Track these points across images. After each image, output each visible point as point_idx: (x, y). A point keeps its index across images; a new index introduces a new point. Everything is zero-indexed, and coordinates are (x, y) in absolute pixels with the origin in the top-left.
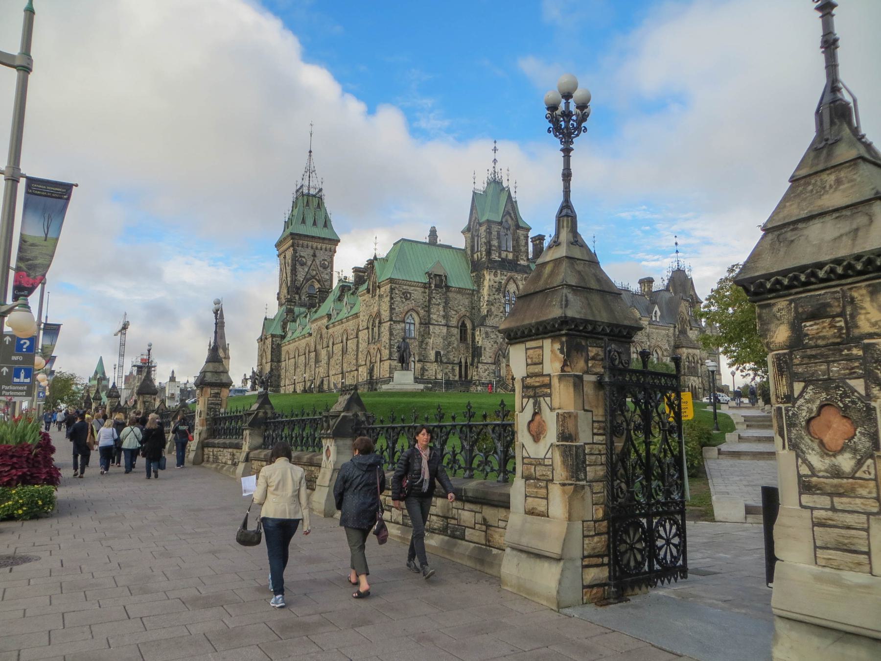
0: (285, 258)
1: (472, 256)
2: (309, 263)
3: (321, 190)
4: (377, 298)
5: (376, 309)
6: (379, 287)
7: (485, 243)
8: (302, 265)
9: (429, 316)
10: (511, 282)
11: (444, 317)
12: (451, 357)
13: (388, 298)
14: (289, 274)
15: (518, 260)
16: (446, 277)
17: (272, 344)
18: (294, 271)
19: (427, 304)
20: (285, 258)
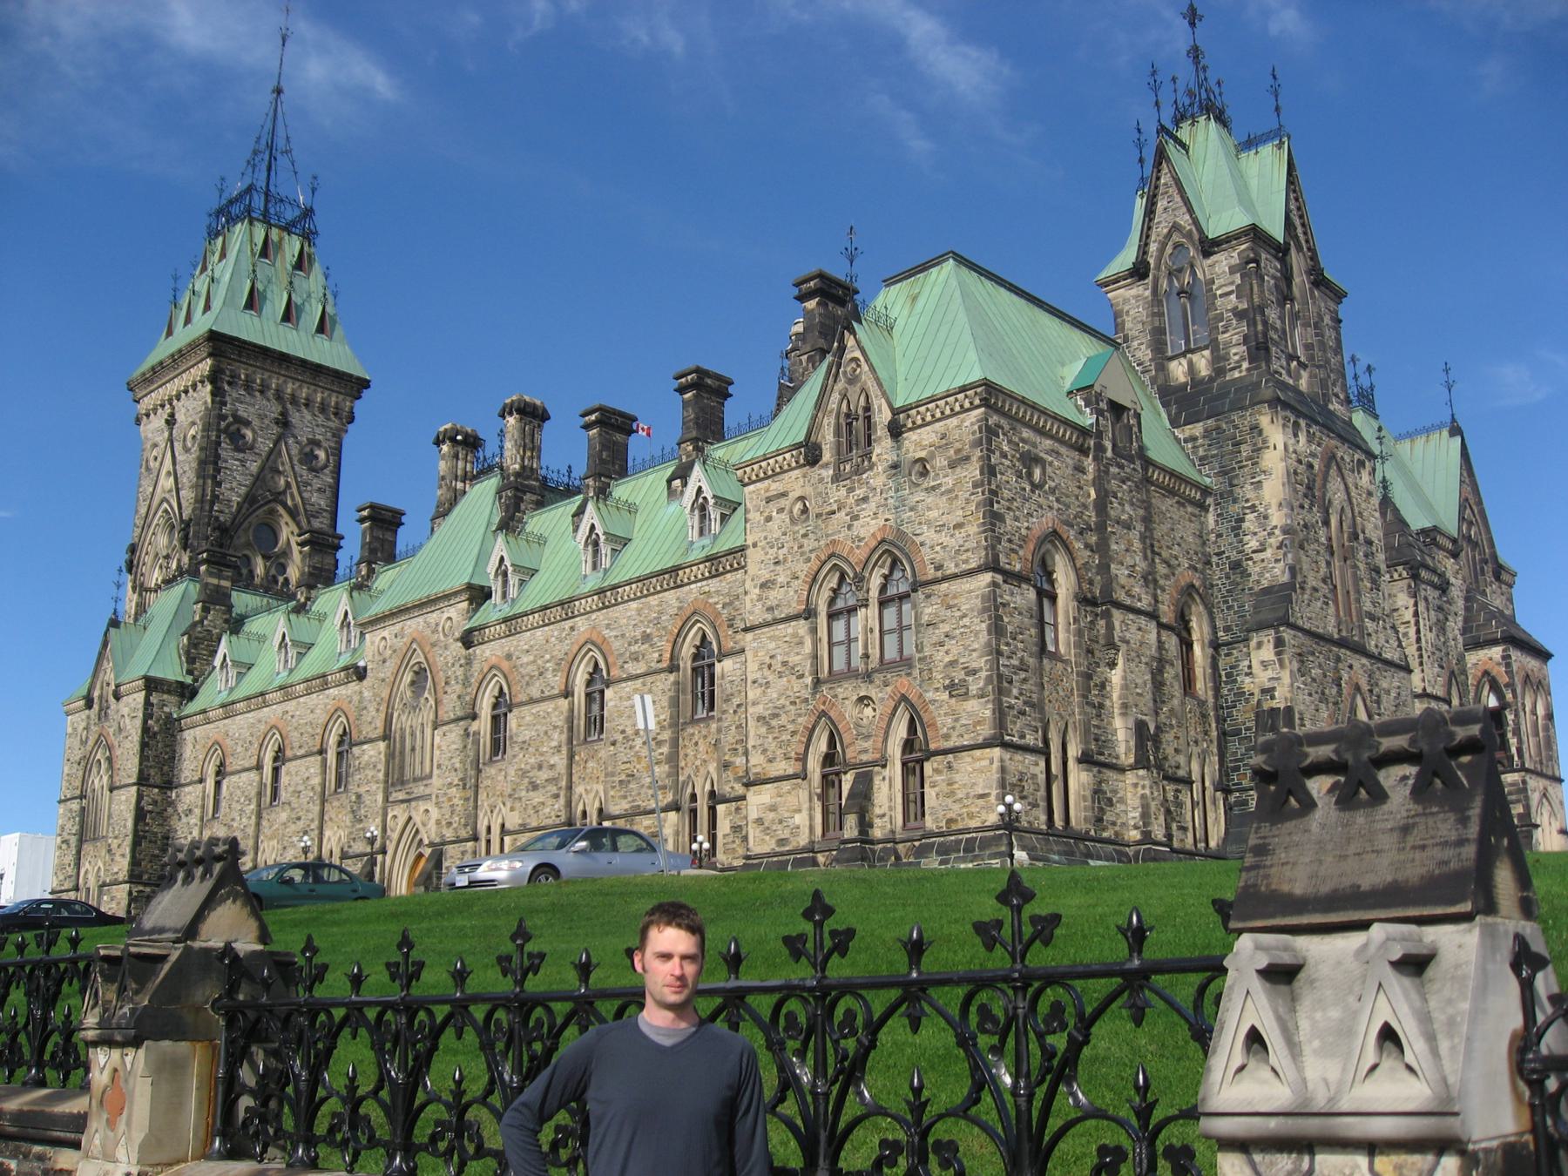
0: (171, 421)
1: (1162, 368)
2: (264, 445)
3: (308, 213)
4: (878, 477)
5: (870, 526)
6: (896, 431)
7: (1240, 315)
8: (238, 449)
9: (1104, 568)
10: (1333, 471)
11: (1149, 579)
12: (1170, 751)
13: (973, 471)
14: (188, 476)
15: (1327, 400)
16: (1138, 416)
17: (147, 716)
18: (210, 465)
19: (1091, 516)
20: (171, 421)
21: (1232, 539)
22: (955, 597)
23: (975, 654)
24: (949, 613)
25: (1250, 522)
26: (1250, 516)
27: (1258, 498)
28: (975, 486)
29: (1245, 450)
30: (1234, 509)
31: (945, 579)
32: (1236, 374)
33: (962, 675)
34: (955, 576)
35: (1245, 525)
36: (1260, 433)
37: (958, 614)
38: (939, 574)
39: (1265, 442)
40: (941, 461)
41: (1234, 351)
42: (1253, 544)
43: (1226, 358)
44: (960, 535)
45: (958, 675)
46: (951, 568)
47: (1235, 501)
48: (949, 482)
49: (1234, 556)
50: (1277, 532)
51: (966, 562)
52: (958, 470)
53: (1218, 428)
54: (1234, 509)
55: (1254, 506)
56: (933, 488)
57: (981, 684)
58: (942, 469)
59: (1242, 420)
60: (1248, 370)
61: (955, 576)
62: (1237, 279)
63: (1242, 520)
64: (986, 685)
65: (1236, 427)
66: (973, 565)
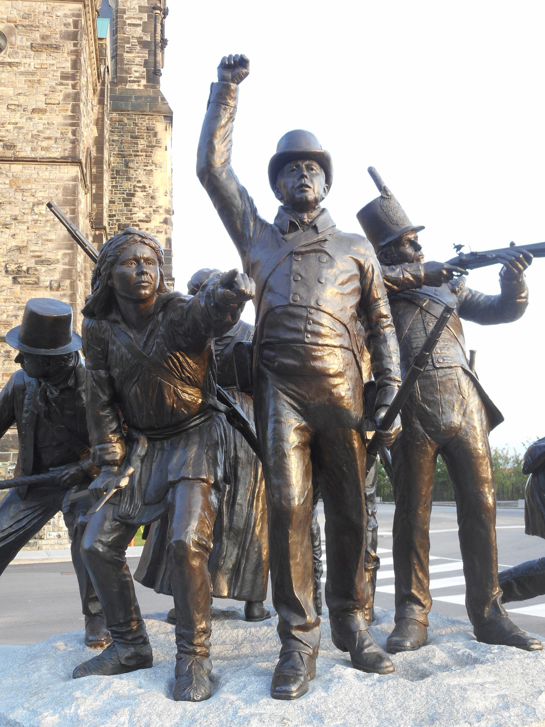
21: (122, 206)
22: (28, 181)
23: (50, 245)
24: (19, 196)
25: (139, 198)
26: (140, 194)
27: (148, 182)
28: (64, 77)
29: (142, 144)
30: (127, 185)
31: (17, 160)
32: (135, 86)
33: (32, 263)
34: (34, 161)
35: (135, 200)
36: (155, 135)
37: (31, 200)
38: (9, 154)
39: (158, 142)
40: (20, 40)
41: (135, 68)
42: (140, 215)
43: (128, 72)
44: (38, 123)
45: (27, 263)
46: (26, 152)
47: (128, 179)
48: (32, 62)
49: (123, 220)
50: (161, 211)
51: (46, 149)
52: (44, 56)
53: (121, 121)
54: (127, 185)
55: (144, 187)
56: (10, 64)
57: (57, 276)
58: (22, 48)
59: (144, 122)
60: (145, 86)
61: (34, 161)
62: (145, 16)
63: (133, 195)
64: (63, 278)
65: (136, 124)
66: (56, 154)
